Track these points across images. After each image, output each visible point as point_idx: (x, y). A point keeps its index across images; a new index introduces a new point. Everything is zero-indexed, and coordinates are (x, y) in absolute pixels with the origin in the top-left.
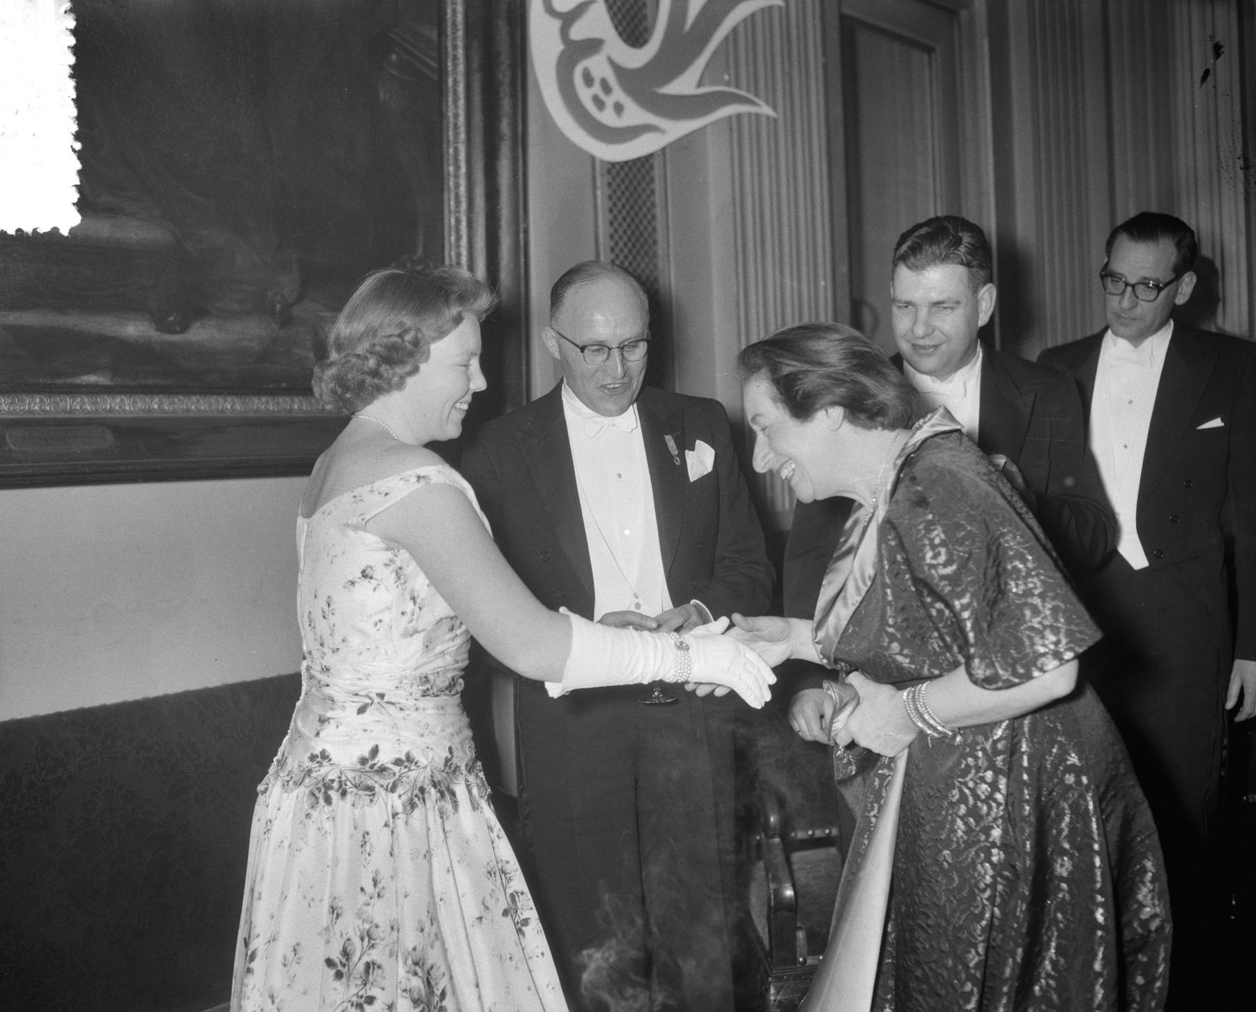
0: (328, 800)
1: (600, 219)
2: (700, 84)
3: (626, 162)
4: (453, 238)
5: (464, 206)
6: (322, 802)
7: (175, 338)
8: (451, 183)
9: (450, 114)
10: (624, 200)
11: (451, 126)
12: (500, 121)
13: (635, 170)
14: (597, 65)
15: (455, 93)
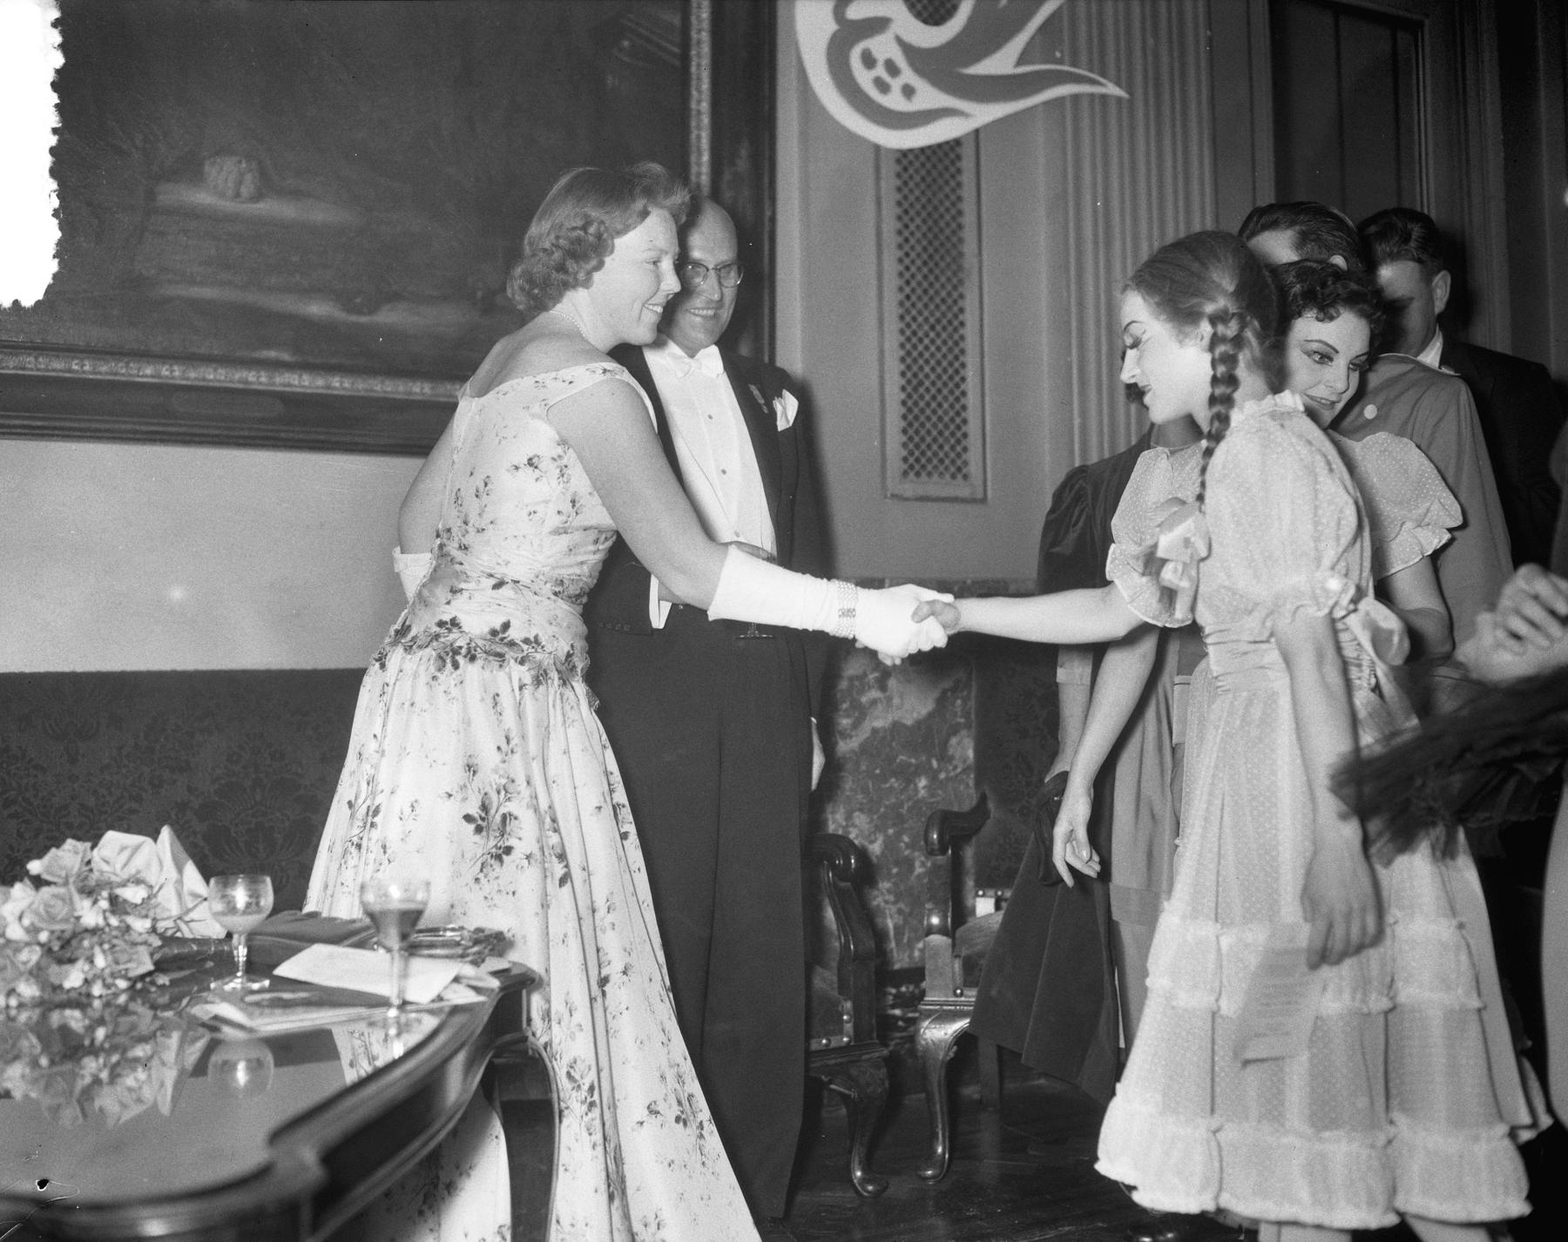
0: (456, 666)
2: (1019, 63)
6: (449, 665)
14: (883, 46)
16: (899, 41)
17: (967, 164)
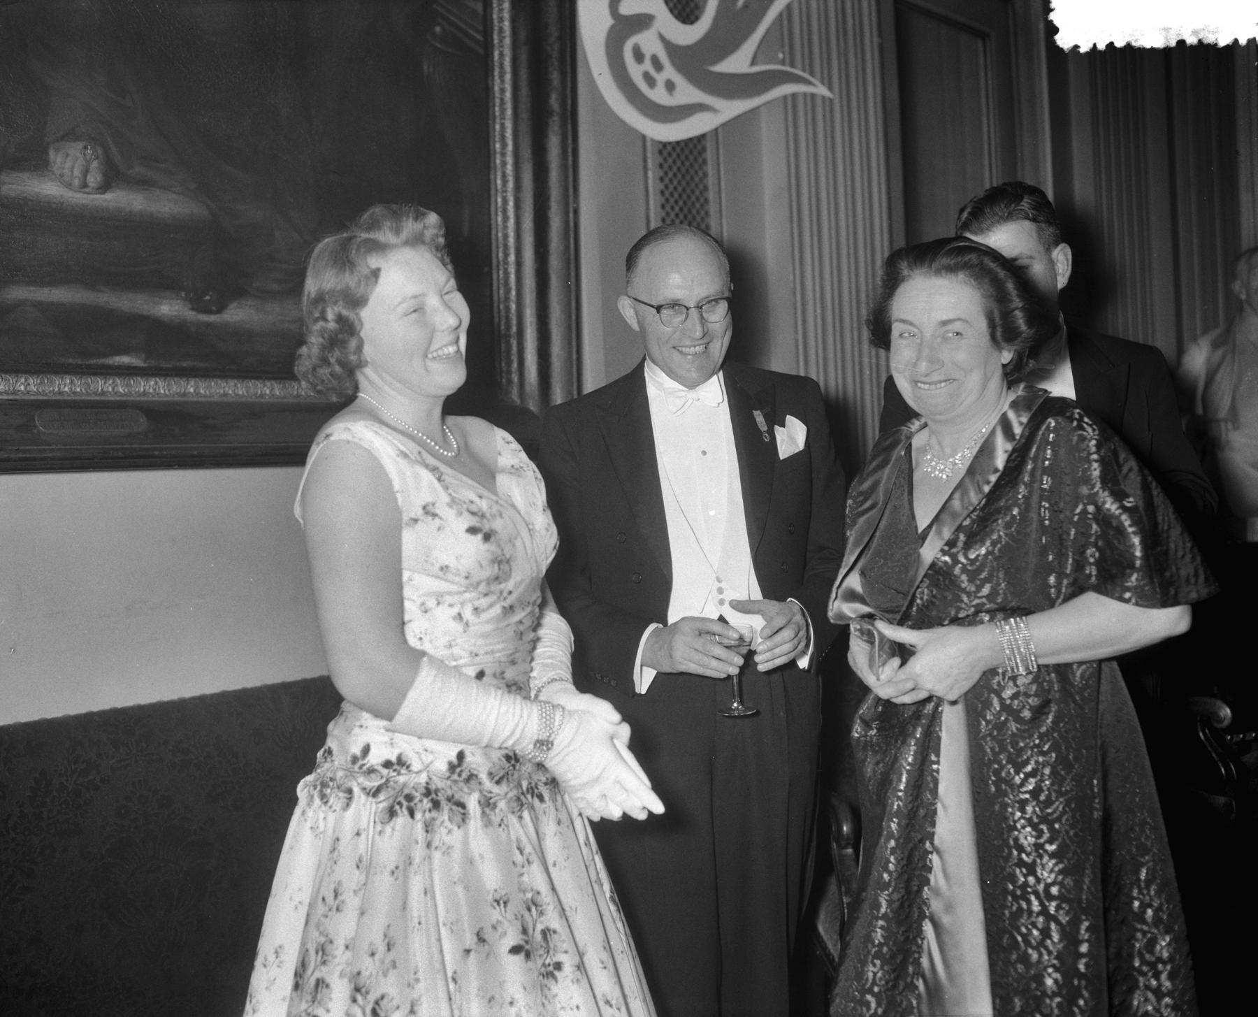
1: (652, 203)
3: (678, 143)
4: (500, 219)
5: (511, 185)
7: (212, 318)
8: (498, 161)
9: (496, 88)
10: (675, 182)
11: (497, 101)
12: (548, 96)
13: (687, 151)
14: (648, 41)
15: (501, 66)
16: (662, 39)
17: (709, 155)
